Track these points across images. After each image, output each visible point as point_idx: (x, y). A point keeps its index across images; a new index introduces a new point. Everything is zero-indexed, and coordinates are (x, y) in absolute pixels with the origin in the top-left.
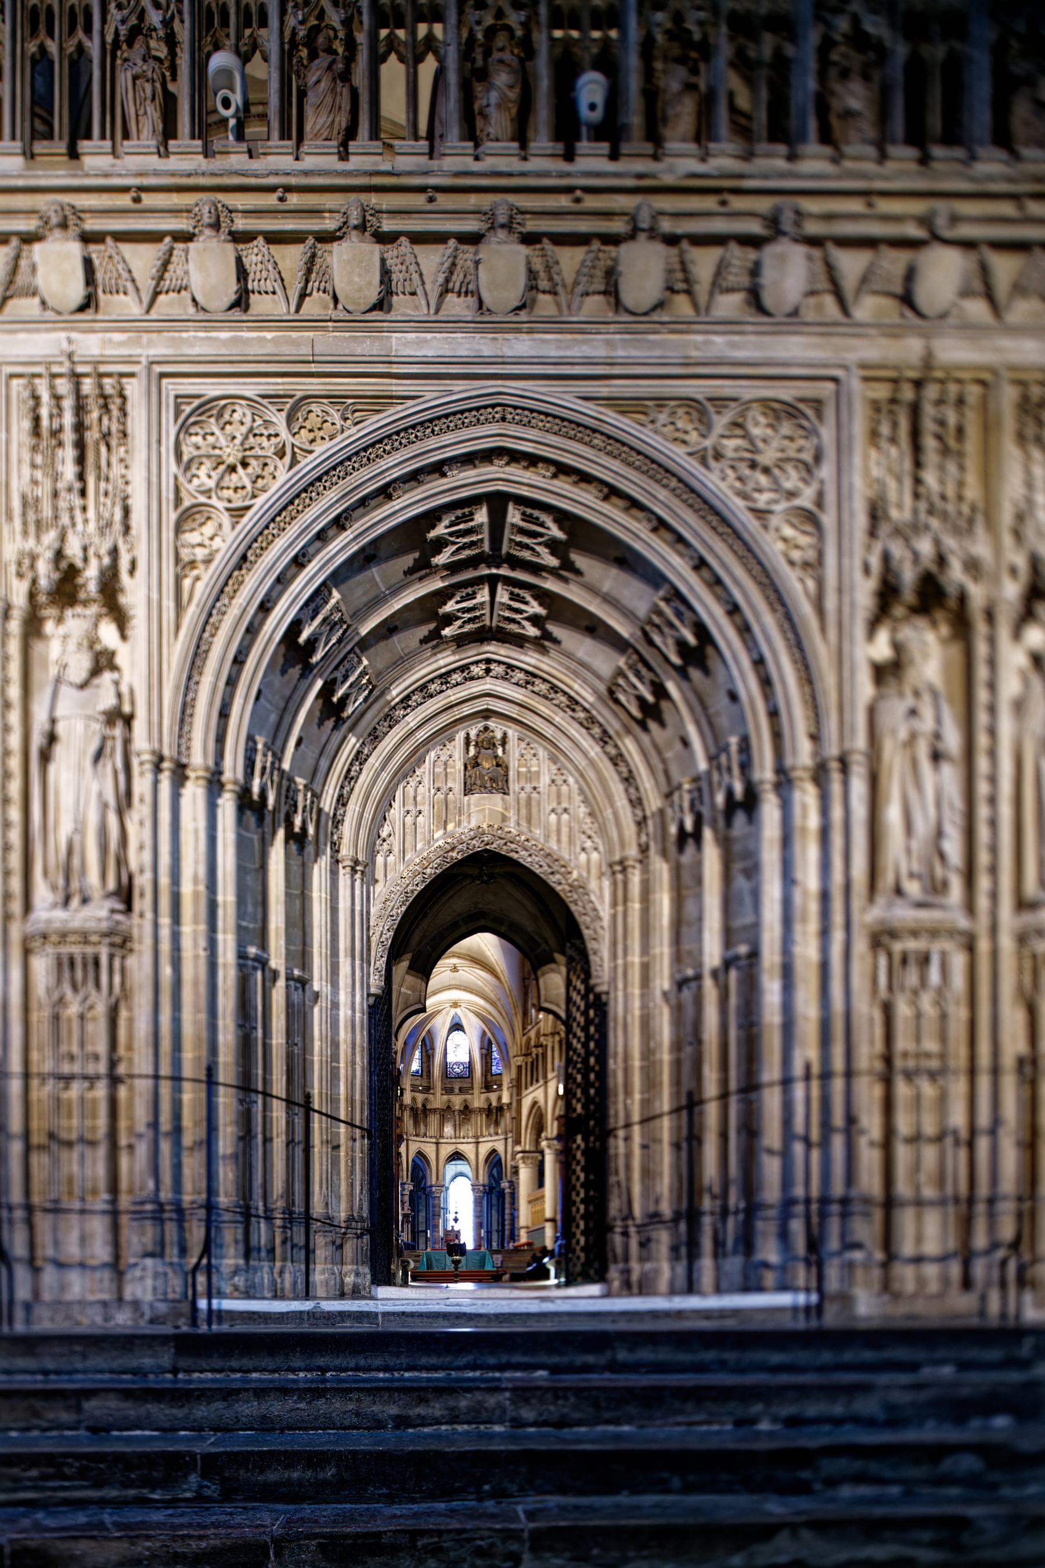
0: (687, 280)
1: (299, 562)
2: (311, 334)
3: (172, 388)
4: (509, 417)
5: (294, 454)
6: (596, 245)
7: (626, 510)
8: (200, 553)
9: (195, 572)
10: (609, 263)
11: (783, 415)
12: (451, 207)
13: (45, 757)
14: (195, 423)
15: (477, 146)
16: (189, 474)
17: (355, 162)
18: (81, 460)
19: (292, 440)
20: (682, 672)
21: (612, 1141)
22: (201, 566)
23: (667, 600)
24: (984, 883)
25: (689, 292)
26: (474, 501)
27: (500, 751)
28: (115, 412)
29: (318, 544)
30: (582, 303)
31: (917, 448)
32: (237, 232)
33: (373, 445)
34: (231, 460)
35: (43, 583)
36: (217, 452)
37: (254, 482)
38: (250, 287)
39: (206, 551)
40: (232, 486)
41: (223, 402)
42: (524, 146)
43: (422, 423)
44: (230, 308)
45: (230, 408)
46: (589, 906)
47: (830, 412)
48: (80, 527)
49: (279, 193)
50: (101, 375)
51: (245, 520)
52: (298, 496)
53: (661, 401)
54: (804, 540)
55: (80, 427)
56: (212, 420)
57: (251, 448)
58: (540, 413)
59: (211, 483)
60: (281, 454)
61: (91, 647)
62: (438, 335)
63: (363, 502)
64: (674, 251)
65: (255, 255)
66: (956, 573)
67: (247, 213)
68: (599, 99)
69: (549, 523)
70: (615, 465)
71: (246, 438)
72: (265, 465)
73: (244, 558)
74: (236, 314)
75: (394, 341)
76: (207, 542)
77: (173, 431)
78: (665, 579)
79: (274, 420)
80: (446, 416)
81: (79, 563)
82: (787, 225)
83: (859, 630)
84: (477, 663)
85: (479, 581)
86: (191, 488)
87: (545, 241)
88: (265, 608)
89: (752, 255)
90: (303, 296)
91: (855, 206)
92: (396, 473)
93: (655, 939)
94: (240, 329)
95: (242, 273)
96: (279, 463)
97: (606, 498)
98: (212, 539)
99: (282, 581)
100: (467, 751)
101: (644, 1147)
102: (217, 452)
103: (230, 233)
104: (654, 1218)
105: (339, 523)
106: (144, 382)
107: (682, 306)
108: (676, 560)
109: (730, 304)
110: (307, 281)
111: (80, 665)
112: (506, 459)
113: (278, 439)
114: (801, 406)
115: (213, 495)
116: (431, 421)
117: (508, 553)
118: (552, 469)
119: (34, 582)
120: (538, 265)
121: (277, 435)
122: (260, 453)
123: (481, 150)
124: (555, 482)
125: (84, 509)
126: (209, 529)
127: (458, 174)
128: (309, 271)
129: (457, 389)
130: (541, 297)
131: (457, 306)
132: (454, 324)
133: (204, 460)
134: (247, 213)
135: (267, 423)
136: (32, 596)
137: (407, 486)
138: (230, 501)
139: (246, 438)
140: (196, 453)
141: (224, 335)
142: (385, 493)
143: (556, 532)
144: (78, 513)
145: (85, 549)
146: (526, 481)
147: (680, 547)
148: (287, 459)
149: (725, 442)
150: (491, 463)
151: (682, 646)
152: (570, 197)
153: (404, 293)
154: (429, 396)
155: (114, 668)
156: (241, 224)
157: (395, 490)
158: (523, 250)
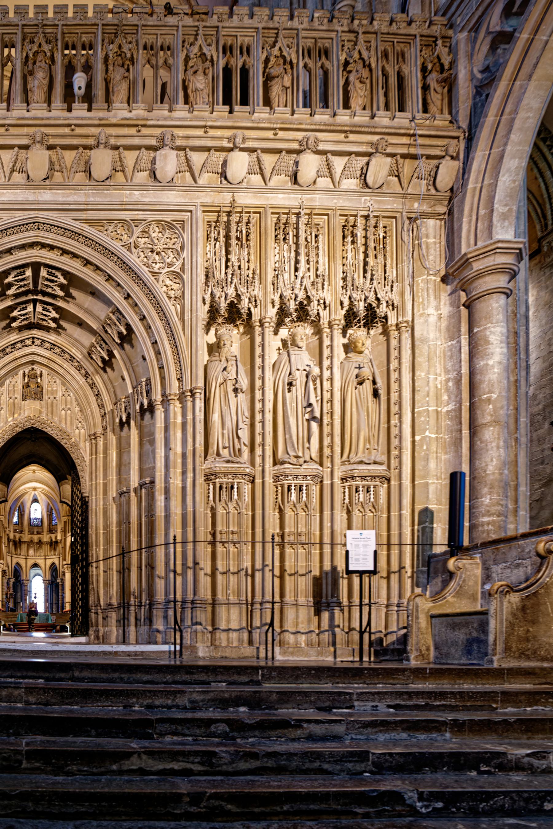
0: (122, 166)
4: (41, 228)
6: (81, 149)
10: (87, 157)
12: (15, 133)
15: (28, 105)
20: (121, 346)
21: (90, 568)
23: (114, 313)
25: (123, 171)
30: (74, 176)
42: (49, 105)
53: (110, 221)
58: (55, 226)
64: (117, 152)
68: (83, 85)
69: (60, 276)
70: (89, 250)
78: (113, 303)
80: (13, 228)
82: (168, 141)
87: (58, 148)
89: (152, 154)
91: (200, 132)
93: (109, 472)
101: (105, 572)
104: (109, 605)
108: (117, 294)
109: (142, 177)
112: (40, 246)
114: (174, 223)
116: (6, 230)
118: (61, 252)
120: (54, 159)
123: (30, 107)
124: (62, 257)
127: (19, 119)
130: (56, 173)
131: (18, 177)
132: (16, 186)
143: (62, 280)
147: (119, 288)
149: (140, 240)
151: (120, 334)
152: (69, 128)
154: (5, 218)
158: (47, 152)
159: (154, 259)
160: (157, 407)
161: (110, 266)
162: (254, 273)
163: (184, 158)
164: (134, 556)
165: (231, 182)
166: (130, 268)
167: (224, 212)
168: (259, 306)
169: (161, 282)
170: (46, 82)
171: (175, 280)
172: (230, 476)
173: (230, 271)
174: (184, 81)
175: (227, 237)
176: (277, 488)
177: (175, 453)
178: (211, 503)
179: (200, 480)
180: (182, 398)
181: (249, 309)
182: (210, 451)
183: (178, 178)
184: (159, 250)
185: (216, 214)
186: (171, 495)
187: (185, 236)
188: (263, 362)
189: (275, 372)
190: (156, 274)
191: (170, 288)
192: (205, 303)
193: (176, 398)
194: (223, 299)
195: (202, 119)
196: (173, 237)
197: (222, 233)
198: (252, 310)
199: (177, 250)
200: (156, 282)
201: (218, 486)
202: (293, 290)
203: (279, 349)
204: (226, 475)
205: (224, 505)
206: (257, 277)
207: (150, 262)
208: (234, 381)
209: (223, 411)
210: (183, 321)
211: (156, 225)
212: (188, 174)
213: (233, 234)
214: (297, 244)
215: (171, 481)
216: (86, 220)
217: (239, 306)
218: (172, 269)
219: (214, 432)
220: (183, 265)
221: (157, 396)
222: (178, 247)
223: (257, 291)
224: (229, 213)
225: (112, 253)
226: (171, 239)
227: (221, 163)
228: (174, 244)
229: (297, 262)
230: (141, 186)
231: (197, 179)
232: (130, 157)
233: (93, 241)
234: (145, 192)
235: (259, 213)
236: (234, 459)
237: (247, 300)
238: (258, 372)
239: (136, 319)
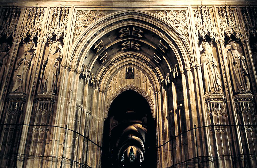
1: (95, 35)
2: (100, 2)
3: (76, 9)
4: (133, 14)
5: (96, 19)
8: (78, 33)
11: (179, 13)
14: (80, 14)
16: (78, 22)
18: (60, 19)
19: (96, 16)
22: (78, 35)
24: (226, 89)
26: (127, 27)
27: (133, 71)
28: (67, 13)
31: (202, 17)
34: (85, 19)
35: (50, 37)
39: (79, 33)
40: (85, 23)
41: (85, 12)
45: (86, 12)
46: (151, 100)
47: (187, 12)
50: (65, 8)
51: (86, 29)
53: (158, 11)
55: (61, 15)
60: (94, 19)
62: (121, 2)
70: (151, 20)
71: (88, 16)
72: (91, 20)
73: (86, 34)
75: (114, 3)
76: (79, 32)
79: (93, 14)
81: (57, 35)
83: (196, 45)
84: (128, 55)
85: (128, 40)
86: (78, 24)
96: (93, 20)
98: (80, 31)
100: (127, 71)
102: (83, 18)
105: (103, 29)
106: (72, 9)
108: (162, 35)
115: (81, 25)
117: (133, 35)
119: (48, 37)
121: (93, 16)
126: (80, 30)
133: (80, 20)
135: (92, 14)
136: (48, 40)
140: (79, 19)
148: (95, 20)
159: (176, 22)
160: (182, 74)
161: (159, 25)
162: (213, 25)
164: (177, 138)
167: (199, 7)
168: (217, 36)
169: (179, 29)
171: (184, 29)
173: (204, 25)
175: (202, 15)
176: (237, 104)
177: (192, 92)
178: (210, 112)
179: (204, 102)
180: (192, 70)
181: (213, 37)
184: (177, 19)
185: (197, 8)
186: (192, 109)
188: (222, 55)
189: (228, 60)
190: (177, 27)
191: (183, 31)
192: (196, 35)
193: (190, 70)
194: (203, 34)
197: (200, 14)
198: (215, 37)
199: (184, 19)
201: (211, 104)
202: (228, 30)
203: (228, 52)
205: (215, 112)
206: (214, 26)
207: (174, 23)
209: (209, 74)
210: (189, 42)
213: (203, 13)
214: (227, 16)
215: (191, 103)
217: (210, 36)
218: (183, 25)
219: (207, 82)
221: (182, 70)
222: (184, 18)
223: (216, 31)
224: (201, 7)
229: (228, 21)
235: (212, 7)
236: (218, 92)
238: (221, 59)
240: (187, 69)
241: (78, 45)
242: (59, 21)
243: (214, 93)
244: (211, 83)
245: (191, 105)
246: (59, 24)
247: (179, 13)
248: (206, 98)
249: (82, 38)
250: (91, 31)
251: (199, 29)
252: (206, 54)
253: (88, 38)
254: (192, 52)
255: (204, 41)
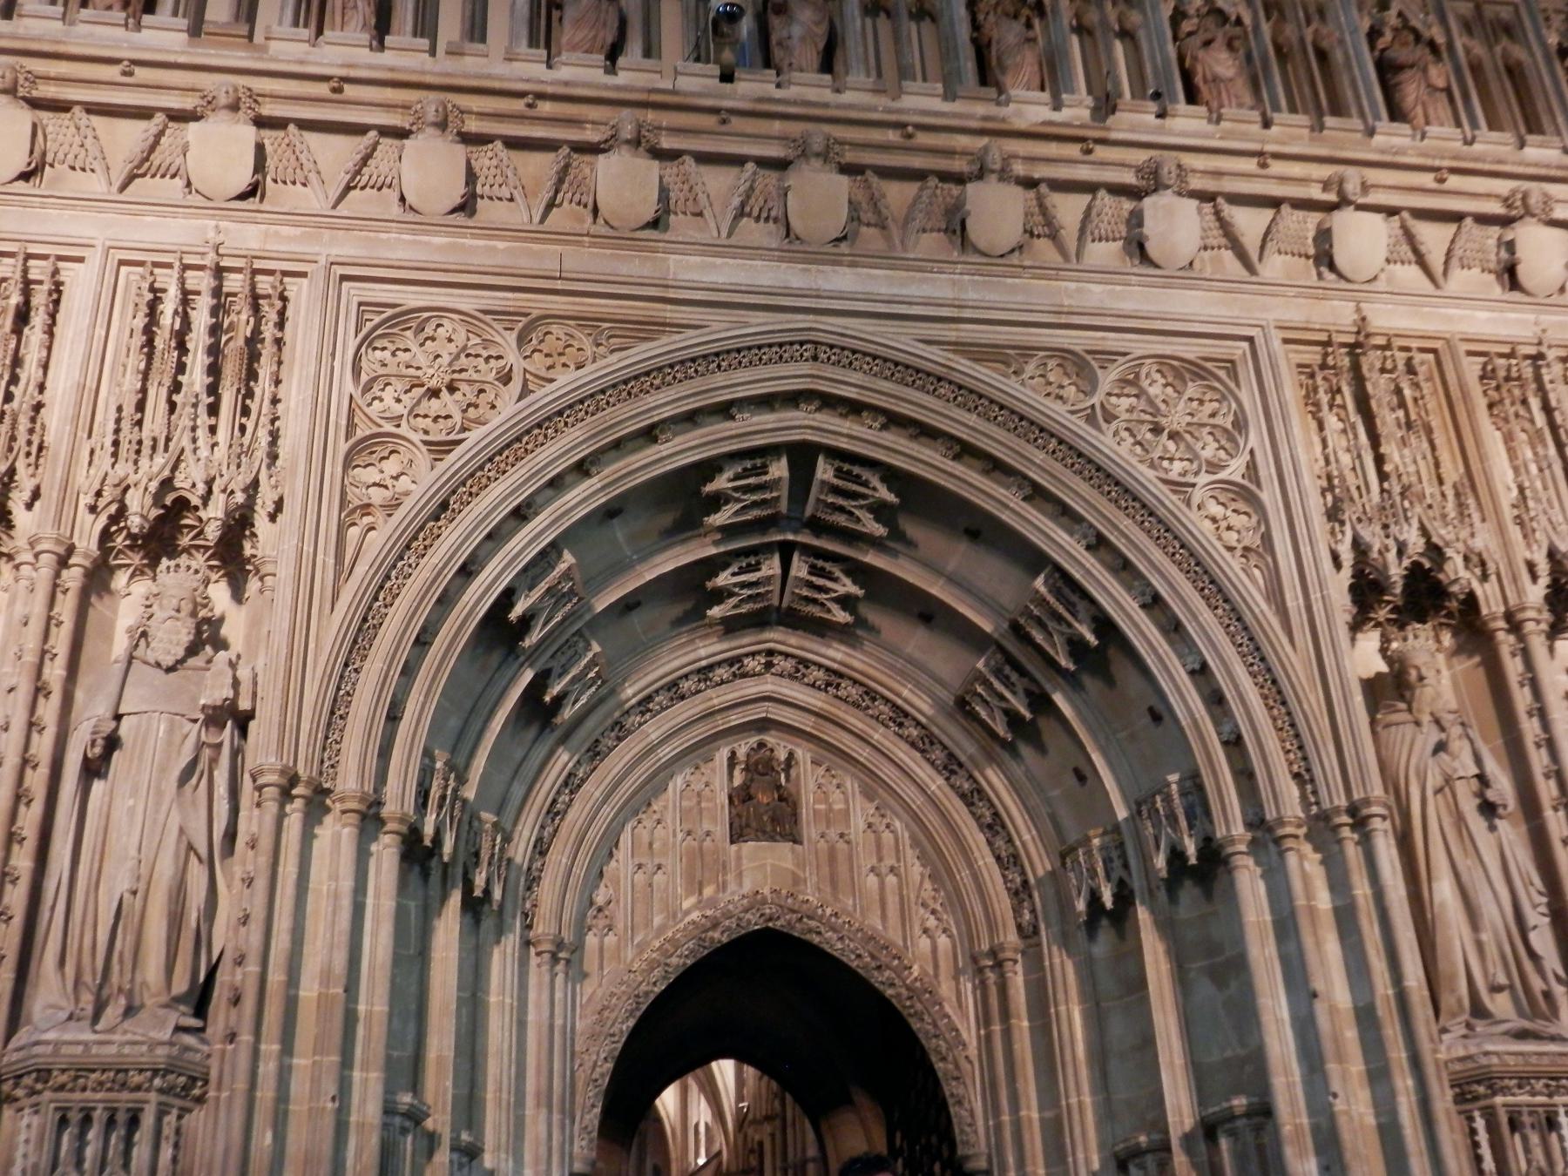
1: (521, 515)
2: (559, 248)
5: (525, 381)
7: (986, 472)
8: (377, 496)
9: (367, 520)
11: (1188, 376)
13: (93, 769)
16: (369, 396)
17: (622, 78)
29: (549, 492)
32: (467, 134)
33: (636, 378)
34: (433, 383)
36: (412, 371)
37: (465, 411)
38: (479, 190)
41: (426, 315)
43: (705, 357)
44: (453, 211)
47: (1247, 373)
48: (204, 452)
49: (529, 99)
52: (528, 432)
53: (1027, 351)
54: (1238, 521)
56: (409, 333)
57: (461, 371)
58: (865, 354)
59: (398, 409)
61: (194, 614)
63: (617, 445)
65: (485, 159)
66: (1457, 572)
67: (482, 115)
70: (972, 419)
71: (457, 357)
72: (481, 391)
74: (460, 219)
77: (352, 345)
79: (498, 339)
80: (739, 351)
88: (467, 571)
89: (1127, 205)
90: (551, 205)
92: (667, 412)
94: (464, 236)
95: (471, 177)
97: (956, 457)
98: (396, 478)
99: (496, 537)
102: (412, 371)
103: (459, 134)
105: (582, 469)
107: (1044, 249)
108: (1062, 537)
109: (1103, 253)
110: (557, 192)
111: (171, 637)
112: (817, 403)
113: (501, 363)
114: (1209, 365)
115: (404, 423)
116: (717, 354)
118: (882, 419)
121: (499, 357)
122: (475, 377)
124: (885, 434)
125: (213, 430)
126: (392, 466)
128: (561, 181)
129: (753, 321)
130: (864, 229)
131: (751, 231)
133: (392, 380)
134: (482, 115)
135: (487, 343)
137: (679, 428)
138: (426, 432)
139: (457, 357)
141: (437, 240)
142: (649, 434)
144: (201, 433)
145: (209, 483)
146: (845, 431)
148: (516, 386)
149: (1113, 400)
150: (797, 407)
153: (685, 213)
154: (715, 326)
155: (221, 644)
156: (473, 126)
157: (662, 432)
159: (1165, 449)
161: (1038, 463)
163: (1213, 218)
165: (1349, 275)
166: (1099, 469)
170: (822, 31)
171: (1234, 505)
172: (1539, 1085)
174: (1181, 59)
182: (1447, 1001)
183: (1202, 260)
184: (1175, 427)
187: (1244, 396)
191: (1223, 524)
195: (1244, 136)
196: (1207, 397)
199: (1225, 430)
200: (1183, 507)
204: (1523, 1080)
208: (1475, 784)
211: (1155, 367)
212: (1228, 255)
216: (956, 344)
217: (1441, 576)
218: (1222, 475)
220: (1252, 467)
223: (1484, 540)
225: (1042, 430)
226: (1201, 402)
227: (1311, 234)
228: (1213, 415)
230: (1104, 274)
231: (1258, 267)
232: (1068, 209)
233: (981, 396)
234: (1118, 288)
237: (1459, 560)
239: (1132, 605)
240: (1281, 822)
241: (382, 589)
242: (213, 390)
243: (1522, 1035)
244: (1480, 946)
245: (1342, 1121)
246: (213, 410)
247: (1188, 376)
248: (1458, 1067)
249: (415, 538)
250: (484, 481)
251: (1359, 520)
252: (1426, 719)
253: (455, 539)
254: (1313, 700)
255: (1389, 602)
